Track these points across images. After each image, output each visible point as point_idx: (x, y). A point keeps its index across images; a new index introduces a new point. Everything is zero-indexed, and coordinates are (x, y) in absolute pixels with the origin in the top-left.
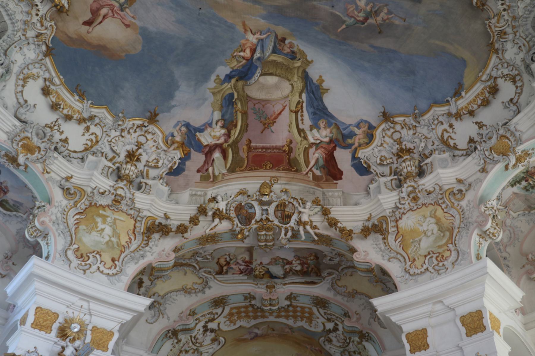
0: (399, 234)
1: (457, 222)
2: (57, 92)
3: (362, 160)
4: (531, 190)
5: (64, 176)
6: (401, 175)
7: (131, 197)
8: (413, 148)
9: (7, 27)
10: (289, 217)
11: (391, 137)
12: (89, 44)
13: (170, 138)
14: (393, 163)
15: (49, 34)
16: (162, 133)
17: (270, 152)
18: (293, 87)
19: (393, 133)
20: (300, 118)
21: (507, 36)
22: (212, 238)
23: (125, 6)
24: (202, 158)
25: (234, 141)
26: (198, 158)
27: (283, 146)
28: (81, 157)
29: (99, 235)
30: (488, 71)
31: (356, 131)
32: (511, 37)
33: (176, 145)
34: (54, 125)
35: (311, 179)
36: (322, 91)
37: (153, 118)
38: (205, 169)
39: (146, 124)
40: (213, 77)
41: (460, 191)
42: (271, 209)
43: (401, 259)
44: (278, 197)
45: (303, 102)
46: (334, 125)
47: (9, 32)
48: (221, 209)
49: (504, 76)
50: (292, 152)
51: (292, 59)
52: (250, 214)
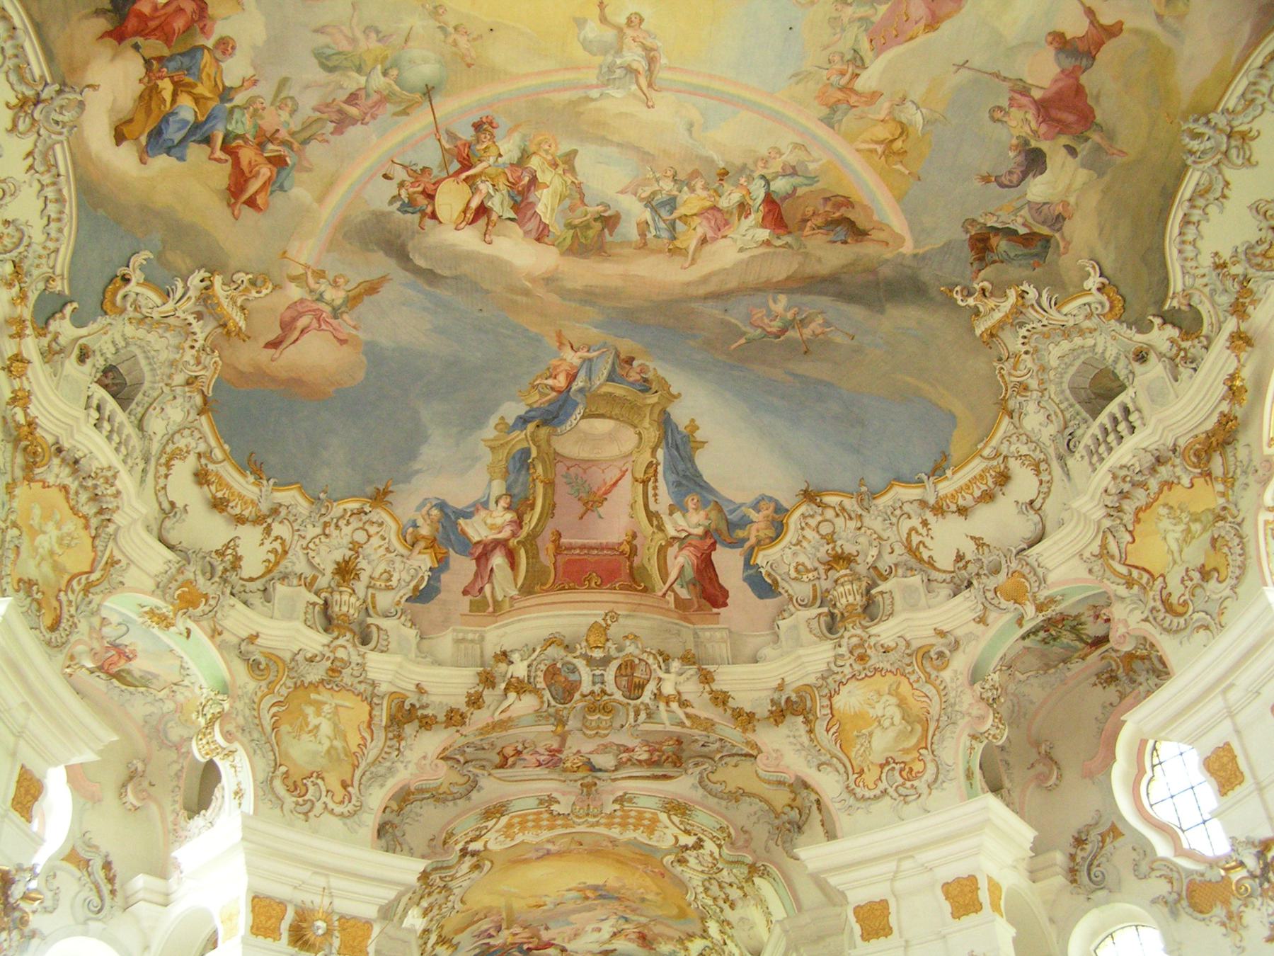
0: (835, 718)
1: (935, 709)
2: (217, 474)
3: (761, 570)
4: (1052, 642)
5: (245, 634)
7: (360, 661)
8: (855, 554)
9: (143, 377)
10: (641, 687)
12: (274, 379)
13: (411, 530)
14: (819, 578)
15: (209, 375)
17: (597, 555)
18: (641, 438)
20: (651, 492)
21: (1029, 394)
22: (502, 725)
23: (343, 309)
24: (471, 566)
25: (528, 535)
26: (462, 568)
27: (621, 544)
28: (262, 588)
29: (313, 738)
30: (994, 443)
31: (753, 515)
32: (1035, 395)
33: (422, 544)
34: (228, 548)
35: (672, 605)
36: (692, 444)
39: (367, 509)
40: (494, 420)
41: (941, 655)
42: (610, 673)
43: (842, 770)
44: (620, 649)
45: (658, 464)
47: (146, 385)
48: (521, 677)
50: (636, 554)
52: (572, 683)
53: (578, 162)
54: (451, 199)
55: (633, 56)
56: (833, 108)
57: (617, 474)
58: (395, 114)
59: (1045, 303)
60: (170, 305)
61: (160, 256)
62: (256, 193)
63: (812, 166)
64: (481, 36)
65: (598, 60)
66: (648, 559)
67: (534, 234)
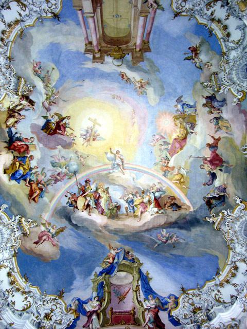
6: (198, 322)
11: (188, 302)
12: (35, 253)
16: (65, 304)
19: (188, 300)
20: (138, 295)
26: (84, 319)
30: (230, 259)
31: (169, 300)
33: (72, 311)
37: (61, 295)
38: (87, 325)
39: (57, 299)
40: (93, 273)
46: (156, 298)
49: (239, 260)
51: (133, 262)
53: (109, 190)
54: (81, 203)
55: (118, 161)
56: (165, 172)
57: (128, 289)
58: (68, 179)
59: (229, 214)
60: (10, 221)
61: (10, 208)
62: (35, 197)
63: (164, 188)
64: (85, 158)
65: (111, 162)
66: (139, 315)
67: (101, 212)
